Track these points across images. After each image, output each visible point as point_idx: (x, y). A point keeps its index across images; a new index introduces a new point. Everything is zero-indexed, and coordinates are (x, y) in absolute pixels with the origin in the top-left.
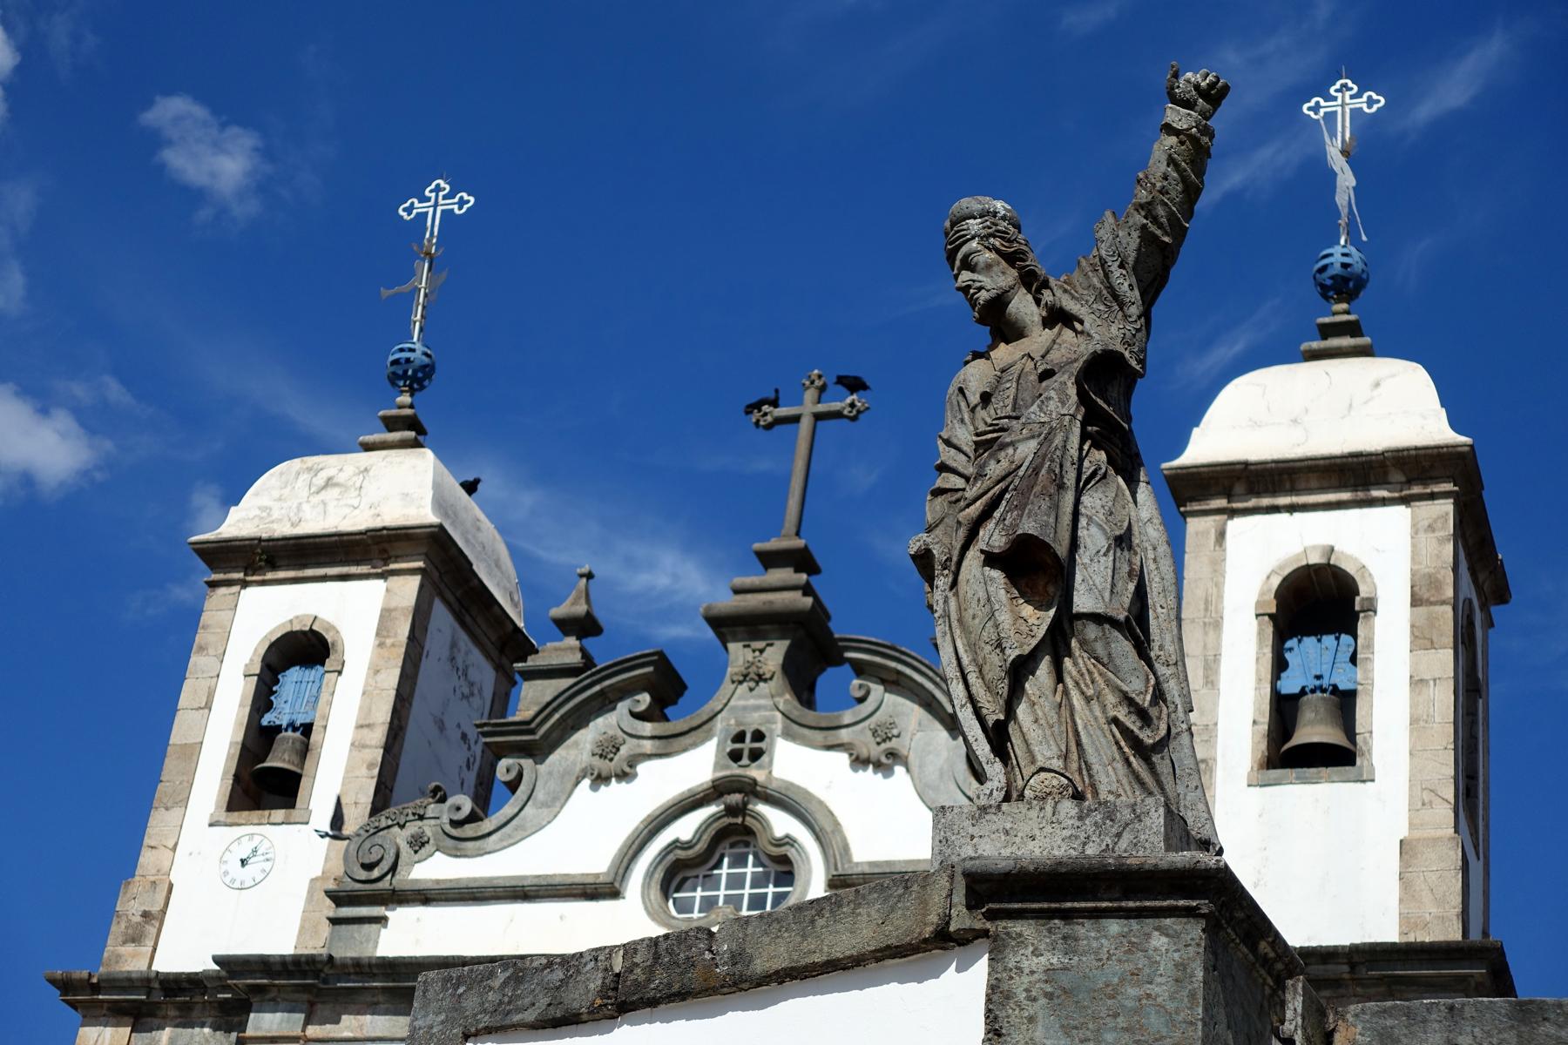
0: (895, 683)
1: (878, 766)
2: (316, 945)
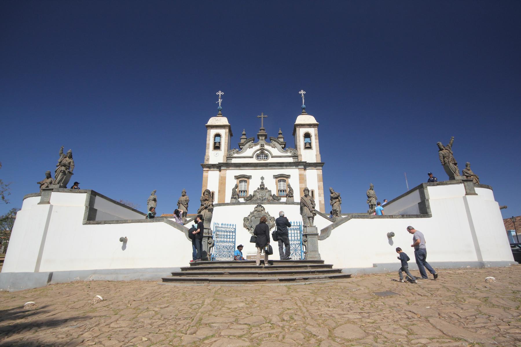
0: (275, 141)
1: (274, 148)
2: (225, 162)
